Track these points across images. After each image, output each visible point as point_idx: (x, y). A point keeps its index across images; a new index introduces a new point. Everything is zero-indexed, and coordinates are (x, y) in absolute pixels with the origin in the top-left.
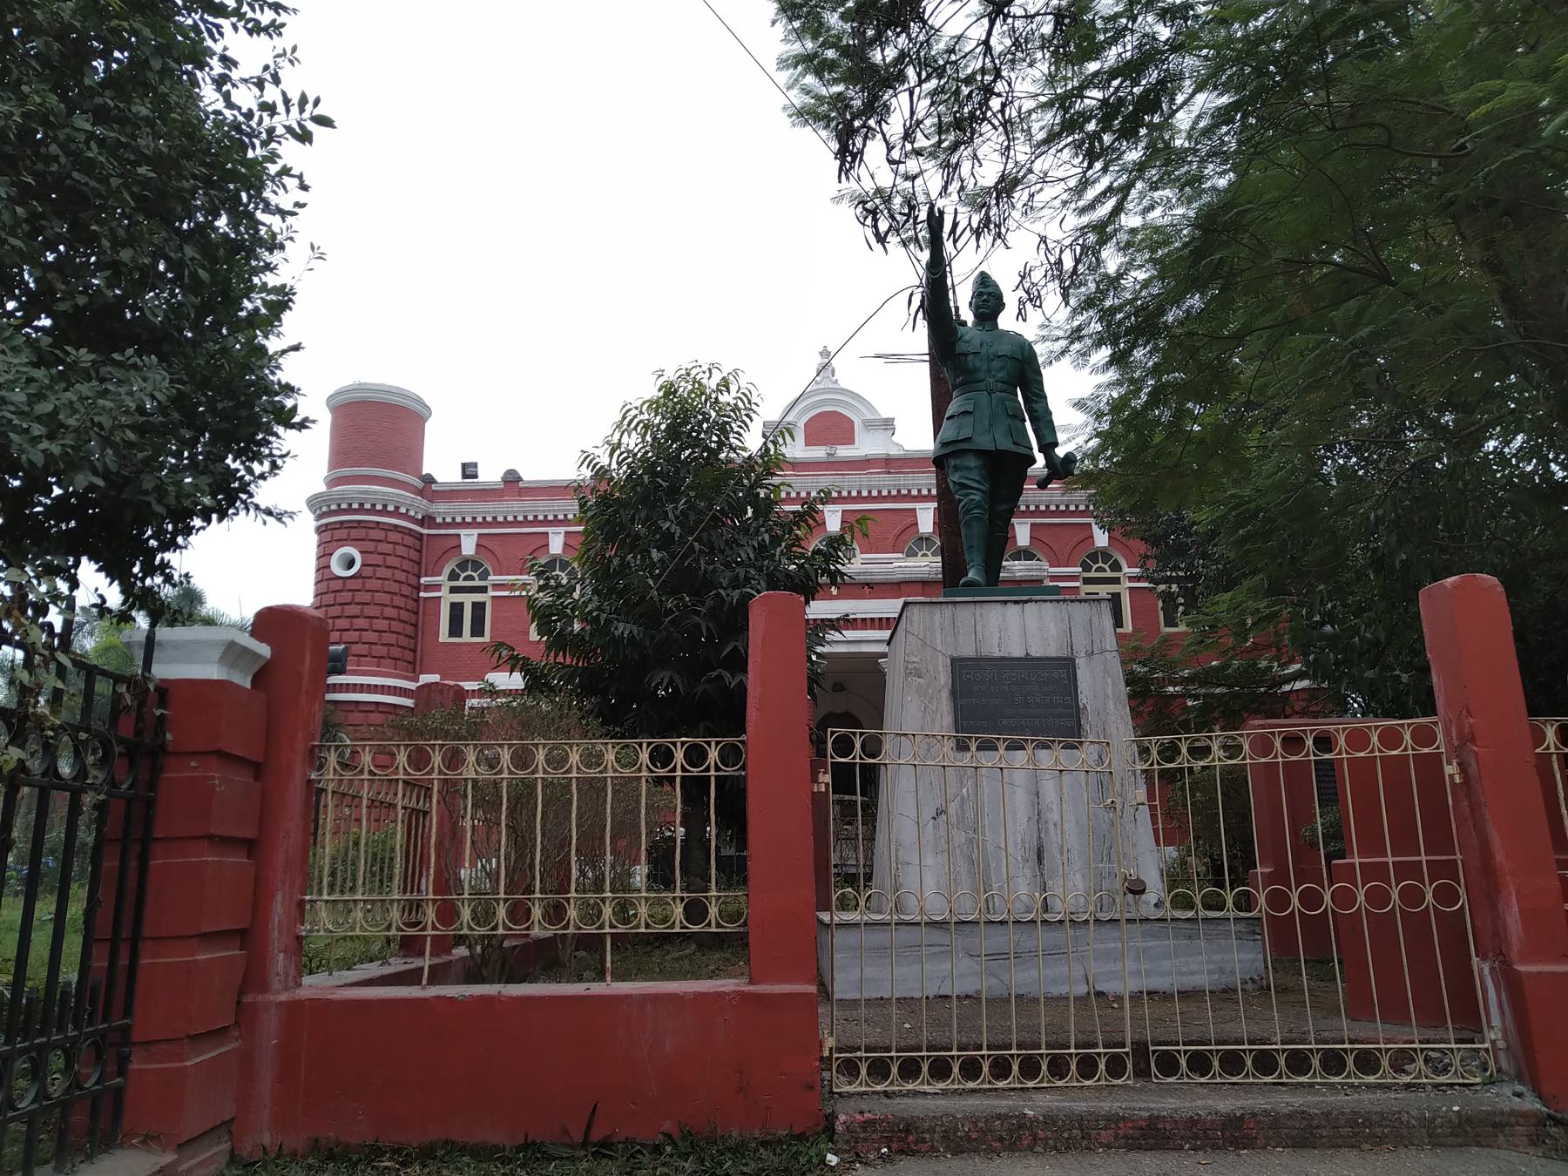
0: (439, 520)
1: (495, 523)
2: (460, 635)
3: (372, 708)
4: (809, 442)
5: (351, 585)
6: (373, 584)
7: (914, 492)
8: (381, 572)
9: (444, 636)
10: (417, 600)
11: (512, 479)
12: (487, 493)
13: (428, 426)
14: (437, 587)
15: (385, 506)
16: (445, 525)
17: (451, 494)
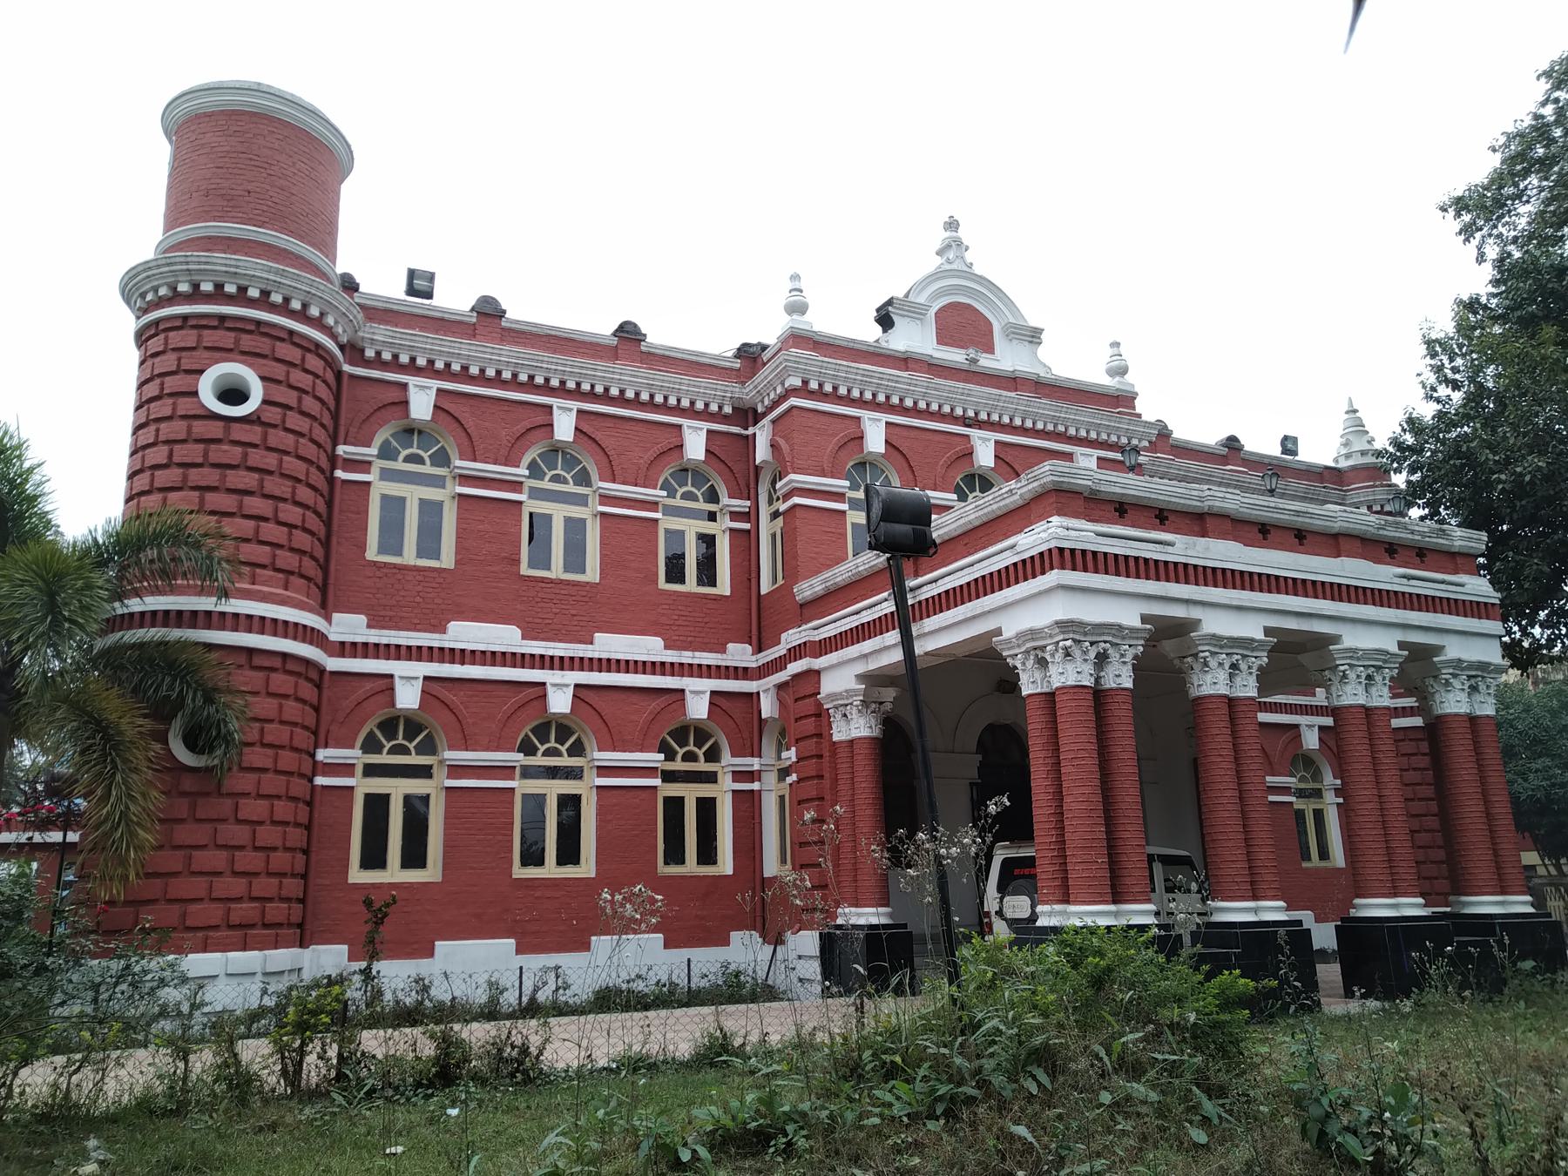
0: (370, 353)
1: (464, 375)
3: (277, 663)
4: (943, 338)
5: (238, 433)
6: (277, 438)
7: (1072, 431)
8: (294, 421)
9: (372, 554)
10: (331, 480)
11: (489, 312)
12: (444, 324)
14: (364, 466)
15: (305, 306)
16: (378, 362)
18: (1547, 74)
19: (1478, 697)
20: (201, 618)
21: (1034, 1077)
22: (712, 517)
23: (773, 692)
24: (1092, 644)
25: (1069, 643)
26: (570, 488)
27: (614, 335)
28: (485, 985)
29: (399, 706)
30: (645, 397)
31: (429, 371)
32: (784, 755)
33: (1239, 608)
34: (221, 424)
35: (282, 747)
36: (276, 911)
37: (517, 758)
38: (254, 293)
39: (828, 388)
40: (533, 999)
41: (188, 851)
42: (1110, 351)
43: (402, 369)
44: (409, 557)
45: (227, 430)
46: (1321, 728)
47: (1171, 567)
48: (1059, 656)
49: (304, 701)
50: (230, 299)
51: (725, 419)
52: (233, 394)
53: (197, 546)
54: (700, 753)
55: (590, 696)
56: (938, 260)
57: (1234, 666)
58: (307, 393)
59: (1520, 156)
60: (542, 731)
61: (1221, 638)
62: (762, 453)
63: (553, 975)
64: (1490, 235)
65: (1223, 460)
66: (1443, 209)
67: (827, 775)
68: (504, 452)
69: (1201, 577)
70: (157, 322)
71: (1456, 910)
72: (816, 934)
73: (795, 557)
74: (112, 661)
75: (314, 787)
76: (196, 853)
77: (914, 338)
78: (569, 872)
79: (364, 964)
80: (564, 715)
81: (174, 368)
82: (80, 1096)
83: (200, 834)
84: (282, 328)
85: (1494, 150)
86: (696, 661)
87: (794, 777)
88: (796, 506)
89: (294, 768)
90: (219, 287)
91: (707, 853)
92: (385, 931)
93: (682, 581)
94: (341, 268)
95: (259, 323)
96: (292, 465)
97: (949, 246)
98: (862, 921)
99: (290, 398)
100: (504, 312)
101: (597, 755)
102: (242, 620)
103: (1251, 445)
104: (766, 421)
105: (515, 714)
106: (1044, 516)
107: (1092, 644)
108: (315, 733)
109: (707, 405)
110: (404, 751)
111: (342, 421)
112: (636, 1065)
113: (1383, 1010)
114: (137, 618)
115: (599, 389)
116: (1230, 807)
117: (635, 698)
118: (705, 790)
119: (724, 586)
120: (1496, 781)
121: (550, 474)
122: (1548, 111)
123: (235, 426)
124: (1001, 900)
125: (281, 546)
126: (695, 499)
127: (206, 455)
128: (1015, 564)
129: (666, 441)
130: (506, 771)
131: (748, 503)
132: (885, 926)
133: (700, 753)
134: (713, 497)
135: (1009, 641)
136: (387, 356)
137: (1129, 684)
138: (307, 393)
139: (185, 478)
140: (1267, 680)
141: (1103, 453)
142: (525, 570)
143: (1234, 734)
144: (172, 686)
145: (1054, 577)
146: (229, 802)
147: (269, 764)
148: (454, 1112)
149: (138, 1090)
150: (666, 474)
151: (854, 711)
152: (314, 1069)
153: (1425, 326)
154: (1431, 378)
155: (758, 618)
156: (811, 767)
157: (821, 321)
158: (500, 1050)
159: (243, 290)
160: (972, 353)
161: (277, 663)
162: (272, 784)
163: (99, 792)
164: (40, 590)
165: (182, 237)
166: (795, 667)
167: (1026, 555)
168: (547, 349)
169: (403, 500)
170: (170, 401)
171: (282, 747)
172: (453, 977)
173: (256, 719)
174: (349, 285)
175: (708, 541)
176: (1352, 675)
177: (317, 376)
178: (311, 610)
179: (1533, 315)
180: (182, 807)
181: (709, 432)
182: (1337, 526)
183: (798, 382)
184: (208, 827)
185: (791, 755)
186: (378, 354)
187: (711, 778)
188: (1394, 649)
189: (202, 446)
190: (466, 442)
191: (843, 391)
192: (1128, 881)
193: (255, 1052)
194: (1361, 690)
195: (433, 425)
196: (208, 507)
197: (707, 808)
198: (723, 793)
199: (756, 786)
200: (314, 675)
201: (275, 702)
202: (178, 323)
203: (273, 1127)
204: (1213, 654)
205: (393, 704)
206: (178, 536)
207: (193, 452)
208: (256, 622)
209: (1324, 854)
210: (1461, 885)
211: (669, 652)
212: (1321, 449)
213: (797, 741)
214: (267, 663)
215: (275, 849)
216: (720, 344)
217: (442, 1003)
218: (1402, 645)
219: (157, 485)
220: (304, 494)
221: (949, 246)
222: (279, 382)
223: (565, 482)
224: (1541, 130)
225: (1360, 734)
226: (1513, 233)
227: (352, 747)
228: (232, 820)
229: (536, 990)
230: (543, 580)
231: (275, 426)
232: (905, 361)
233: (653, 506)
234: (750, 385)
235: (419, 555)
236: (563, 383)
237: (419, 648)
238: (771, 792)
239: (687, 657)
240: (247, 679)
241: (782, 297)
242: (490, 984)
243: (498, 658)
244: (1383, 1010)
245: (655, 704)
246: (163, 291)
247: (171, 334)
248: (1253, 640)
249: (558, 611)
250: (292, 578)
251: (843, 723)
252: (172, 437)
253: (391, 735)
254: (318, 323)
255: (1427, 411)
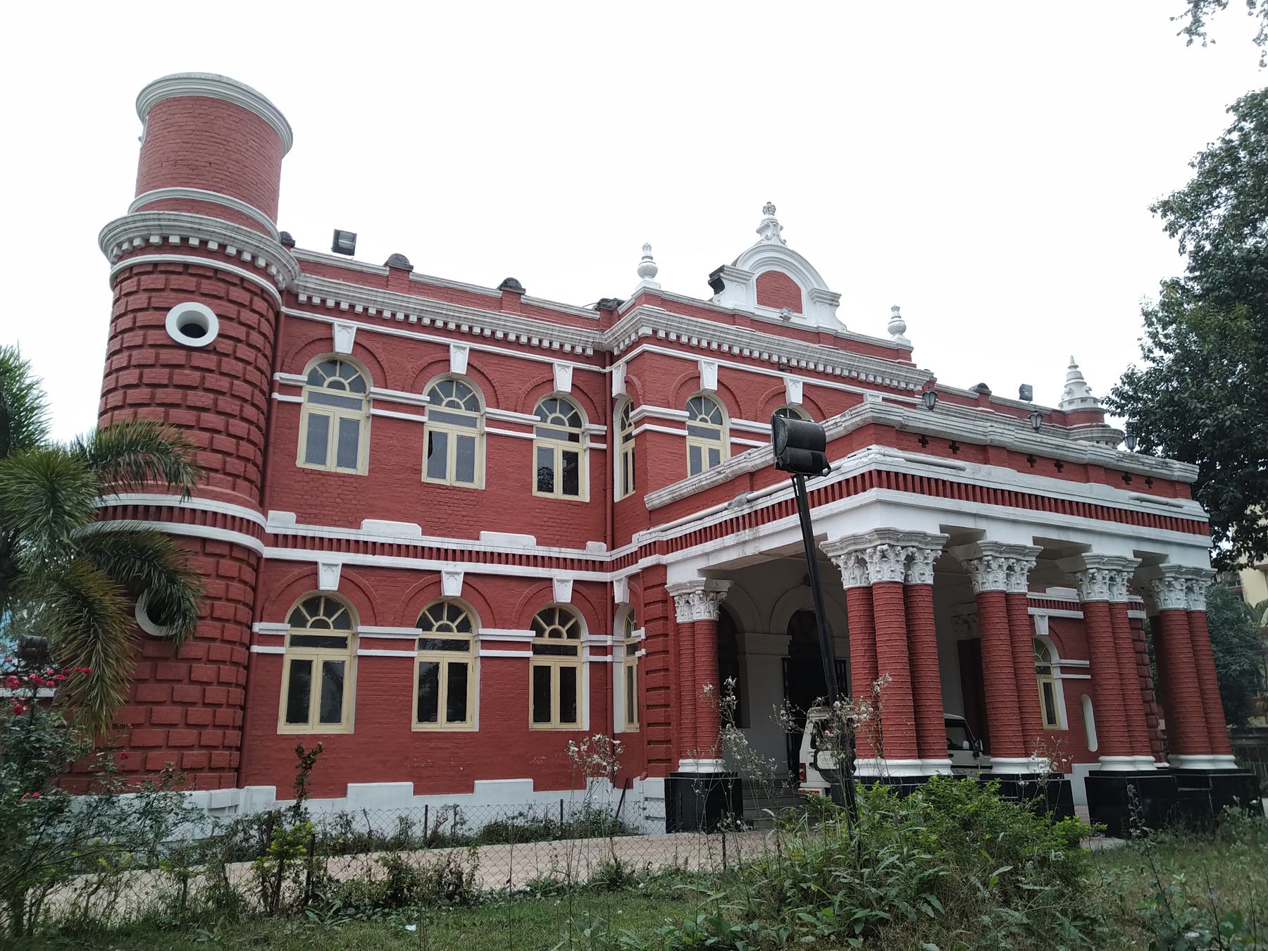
0: (303, 298)
1: (378, 318)
2: (324, 463)
3: (226, 551)
4: (762, 300)
5: (198, 360)
6: (229, 365)
7: (863, 377)
8: (243, 351)
9: (301, 462)
10: (270, 401)
11: (399, 267)
12: (362, 275)
13: (289, 165)
14: (295, 389)
15: (254, 258)
17: (312, 265)
18: (1235, 109)
19: (1193, 596)
20: (164, 512)
21: (929, 904)
22: (574, 438)
23: (625, 582)
24: (903, 548)
25: (885, 547)
26: (463, 412)
27: (500, 288)
28: (398, 822)
29: (322, 588)
30: (524, 339)
31: (351, 313)
32: (634, 633)
33: (1014, 522)
34: (184, 352)
35: (228, 621)
36: (221, 757)
37: (418, 633)
38: (213, 246)
39: (673, 337)
40: (435, 832)
41: (149, 706)
42: (892, 314)
43: (328, 311)
44: (331, 465)
45: (189, 357)
46: (1050, 618)
47: (963, 487)
48: (877, 557)
49: (245, 583)
50: (193, 251)
51: (587, 359)
52: (193, 328)
53: (165, 452)
54: (564, 630)
55: (478, 584)
56: (758, 238)
57: (1010, 568)
58: (253, 328)
59: (1213, 171)
60: (436, 611)
61: (1002, 545)
62: (618, 387)
63: (452, 812)
64: (1189, 232)
65: (976, 403)
66: (1153, 210)
67: (672, 650)
68: (410, 381)
69: (992, 496)
70: (131, 268)
71: (1175, 765)
72: (662, 780)
73: (646, 473)
74: (94, 546)
75: (250, 654)
76: (155, 708)
77: (739, 298)
78: (457, 727)
79: (293, 802)
80: (455, 598)
81: (145, 305)
82: (97, 912)
83: (160, 692)
84: (236, 275)
85: (1193, 166)
86: (562, 556)
87: (643, 652)
88: (646, 431)
89: (237, 639)
90: (185, 240)
91: (568, 713)
92: (312, 775)
93: (551, 490)
94: (281, 227)
95: (216, 270)
96: (241, 388)
97: (767, 226)
98: (703, 770)
99: (241, 332)
100: (412, 267)
101: (482, 631)
102: (198, 515)
103: (997, 391)
104: (621, 362)
105: (415, 596)
106: (864, 444)
107: (903, 548)
108: (253, 609)
109: (573, 348)
110: (324, 625)
111: (279, 353)
112: (546, 889)
113: (1128, 846)
114: (110, 511)
115: (487, 332)
116: (1007, 681)
117: (512, 584)
118: (567, 661)
119: (584, 494)
120: (1207, 663)
121: (446, 400)
122: (1235, 136)
123: (195, 354)
124: (816, 753)
125: (230, 454)
126: (563, 423)
127: (171, 378)
128: (840, 483)
129: (539, 376)
130: (407, 643)
131: (605, 428)
132: (716, 775)
133: (564, 630)
134: (575, 421)
135: (833, 544)
136: (316, 300)
137: (930, 581)
138: (253, 328)
139: (153, 396)
140: (1038, 579)
141: (886, 395)
142: (425, 478)
143: (1010, 623)
144: (141, 566)
145: (873, 494)
146: (184, 666)
147: (217, 634)
148: (412, 928)
149: (144, 907)
150: (540, 403)
151: (696, 598)
152: (289, 891)
153: (1144, 301)
154: (1149, 342)
155: (613, 522)
156: (658, 643)
157: (668, 283)
158: (441, 876)
159: (204, 243)
160: (785, 312)
161: (226, 551)
162: (220, 650)
163: (82, 657)
164: (43, 486)
165: (153, 199)
166: (645, 562)
167: (849, 476)
168: (445, 299)
169: (327, 418)
170: (142, 332)
171: (228, 621)
172: (371, 814)
173: (207, 597)
174: (288, 242)
175: (571, 458)
176: (1099, 577)
177: (261, 315)
178: (253, 508)
179: (1228, 295)
180: (146, 669)
181: (575, 369)
182: (1087, 458)
183: (650, 332)
184: (166, 686)
185: (641, 633)
186: (310, 298)
187: (572, 651)
188: (1131, 556)
189: (167, 370)
190: (379, 373)
191: (684, 339)
192: (931, 740)
193: (241, 875)
194: (1105, 588)
195: (353, 358)
196: (172, 420)
197: (568, 676)
198: (582, 664)
199: (608, 658)
200: (253, 561)
201: (223, 583)
202: (147, 270)
203: (266, 940)
204: (995, 558)
205: (317, 587)
206: (149, 443)
207: (160, 375)
208: (209, 517)
209: (1052, 720)
210: (1173, 744)
211: (541, 548)
212: (1049, 397)
213: (646, 622)
214: (218, 551)
215: (220, 705)
216: (583, 298)
217: (360, 836)
218: (1136, 554)
219: (128, 401)
220: (250, 412)
221: (767, 226)
222: (231, 319)
223: (458, 407)
224: (1230, 152)
225: (1105, 624)
226: (1206, 232)
227: (283, 621)
228: (186, 681)
229: (437, 827)
230: (439, 486)
231: (227, 355)
232: (733, 317)
233: (528, 428)
234: (608, 333)
235: (339, 464)
236: (458, 326)
237: (339, 540)
238: (621, 663)
239: (555, 552)
240: (201, 563)
241: (636, 263)
242: (401, 820)
243: (403, 550)
244: (1128, 846)
245: (528, 590)
246: (137, 242)
247: (143, 277)
248: (1025, 547)
249: (451, 512)
250: (239, 481)
251: (686, 608)
252: (143, 362)
253: (314, 613)
254: (264, 272)
255: (1143, 367)
